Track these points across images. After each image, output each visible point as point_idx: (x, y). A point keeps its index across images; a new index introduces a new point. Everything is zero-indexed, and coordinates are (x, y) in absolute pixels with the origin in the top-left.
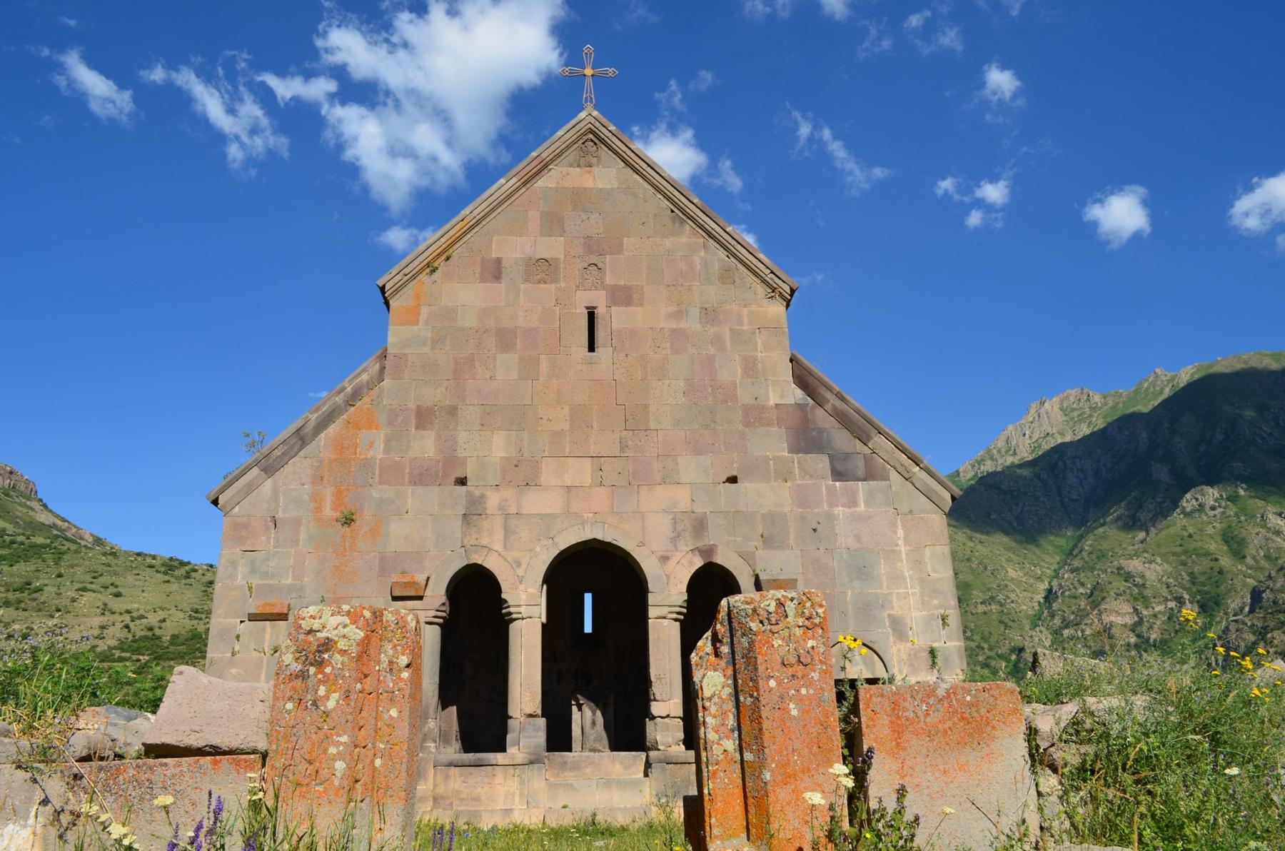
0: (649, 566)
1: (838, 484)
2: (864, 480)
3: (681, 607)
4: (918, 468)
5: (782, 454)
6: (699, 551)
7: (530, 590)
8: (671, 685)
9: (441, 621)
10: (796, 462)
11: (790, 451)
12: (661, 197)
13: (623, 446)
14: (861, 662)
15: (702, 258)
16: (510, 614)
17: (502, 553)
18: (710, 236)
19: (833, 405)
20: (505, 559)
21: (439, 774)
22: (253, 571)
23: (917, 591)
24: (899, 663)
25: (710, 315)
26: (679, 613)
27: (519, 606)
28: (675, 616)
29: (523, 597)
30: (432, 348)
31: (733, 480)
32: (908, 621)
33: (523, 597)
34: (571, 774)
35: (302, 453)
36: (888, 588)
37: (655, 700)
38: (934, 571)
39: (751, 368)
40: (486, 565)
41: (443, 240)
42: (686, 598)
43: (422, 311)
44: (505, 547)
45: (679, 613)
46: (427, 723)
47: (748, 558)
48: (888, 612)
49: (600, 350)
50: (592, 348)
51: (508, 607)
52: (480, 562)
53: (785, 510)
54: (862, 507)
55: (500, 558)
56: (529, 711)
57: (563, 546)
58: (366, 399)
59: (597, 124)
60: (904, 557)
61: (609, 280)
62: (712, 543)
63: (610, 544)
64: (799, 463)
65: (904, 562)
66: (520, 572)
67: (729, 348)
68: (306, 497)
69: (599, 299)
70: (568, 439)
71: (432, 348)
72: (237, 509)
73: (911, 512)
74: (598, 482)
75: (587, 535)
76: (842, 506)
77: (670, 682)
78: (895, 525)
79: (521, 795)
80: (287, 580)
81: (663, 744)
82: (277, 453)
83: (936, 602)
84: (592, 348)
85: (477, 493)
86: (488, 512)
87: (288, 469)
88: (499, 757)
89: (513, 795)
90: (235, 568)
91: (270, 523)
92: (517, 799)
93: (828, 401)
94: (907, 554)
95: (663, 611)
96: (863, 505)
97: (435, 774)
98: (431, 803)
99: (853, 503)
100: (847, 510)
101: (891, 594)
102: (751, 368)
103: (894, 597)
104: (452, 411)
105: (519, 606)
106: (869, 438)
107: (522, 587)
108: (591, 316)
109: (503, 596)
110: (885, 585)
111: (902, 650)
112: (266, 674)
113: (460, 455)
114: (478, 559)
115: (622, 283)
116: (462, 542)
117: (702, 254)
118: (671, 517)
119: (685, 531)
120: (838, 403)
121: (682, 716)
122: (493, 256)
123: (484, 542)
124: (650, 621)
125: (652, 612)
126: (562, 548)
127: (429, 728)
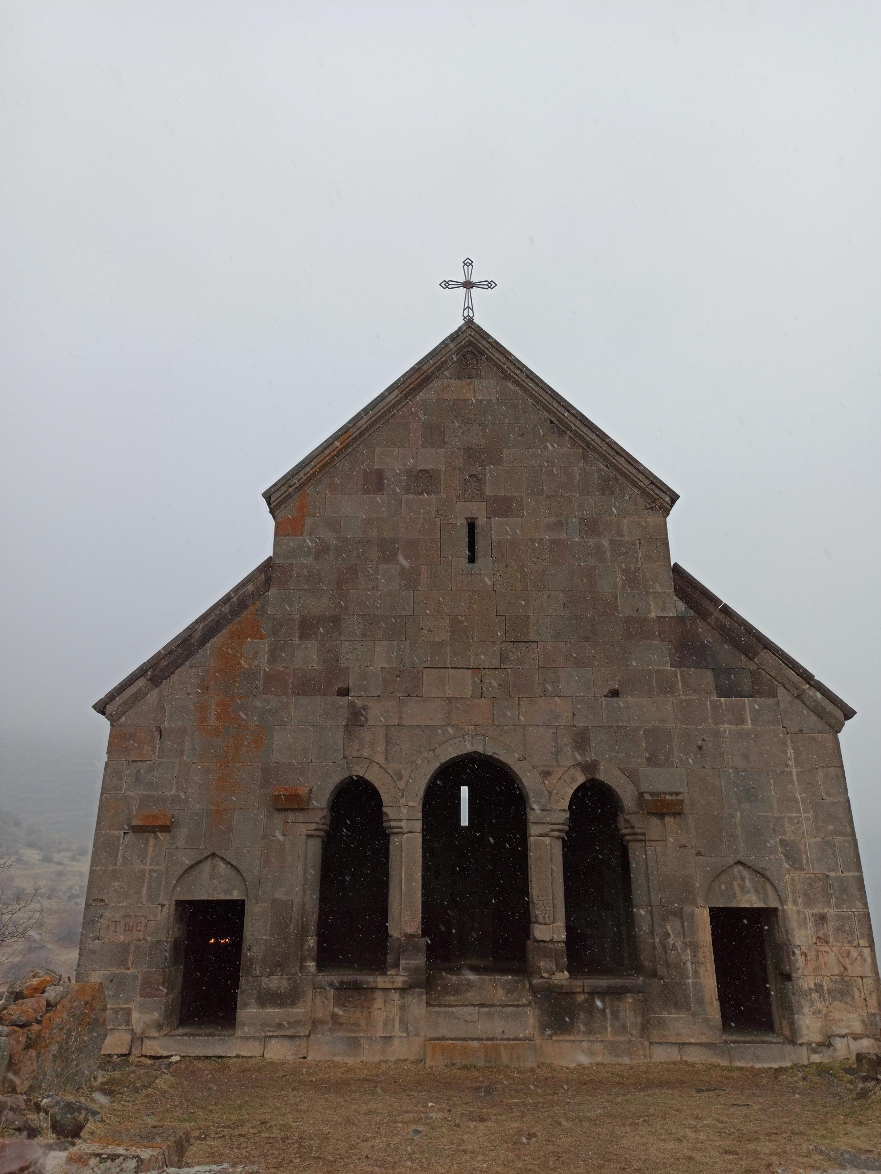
0: (529, 780)
1: (722, 699)
2: (751, 696)
3: (563, 824)
4: (807, 686)
5: (664, 668)
7: (411, 804)
8: (554, 908)
10: (679, 677)
11: (672, 666)
12: (540, 408)
13: (504, 658)
14: (752, 891)
15: (581, 468)
16: (391, 828)
17: (383, 765)
18: (589, 447)
19: (717, 619)
20: (387, 772)
21: (318, 997)
22: (138, 780)
23: (811, 815)
24: (794, 892)
25: (590, 526)
28: (557, 834)
29: (405, 811)
30: (316, 558)
31: (615, 693)
32: (802, 847)
33: (405, 811)
34: (452, 998)
35: (187, 663)
36: (780, 812)
37: (537, 922)
38: (828, 794)
39: (632, 579)
40: (367, 777)
41: (327, 452)
42: (568, 816)
43: (307, 522)
44: (386, 759)
45: (560, 831)
46: (307, 941)
47: (632, 776)
48: (780, 837)
49: (480, 561)
50: (472, 559)
51: (390, 820)
53: (669, 726)
54: (749, 725)
56: (410, 931)
57: (444, 758)
58: (251, 609)
59: (477, 336)
60: (795, 778)
61: (489, 491)
63: (491, 757)
64: (681, 677)
65: (796, 784)
66: (401, 785)
67: (609, 559)
68: (192, 707)
69: (479, 511)
70: (448, 649)
71: (315, 559)
72: (123, 719)
73: (801, 731)
74: (479, 694)
75: (468, 747)
76: (729, 723)
78: (784, 744)
79: (402, 1021)
80: (171, 790)
81: (547, 972)
82: (164, 663)
83: (831, 828)
84: (472, 559)
85: (359, 703)
86: (370, 722)
87: (175, 677)
88: (381, 981)
89: (394, 1019)
90: (120, 779)
91: (156, 733)
92: (397, 1025)
93: (711, 614)
94: (797, 775)
95: (546, 829)
96: (750, 722)
99: (741, 720)
100: (733, 727)
101: (783, 818)
102: (632, 579)
103: (786, 820)
104: (336, 621)
105: (400, 820)
106: (756, 654)
107: (403, 801)
108: (472, 527)
109: (384, 809)
110: (776, 807)
111: (797, 879)
112: (149, 888)
113: (342, 666)
114: (359, 771)
115: (502, 494)
117: (582, 465)
118: (552, 731)
119: (566, 745)
120: (722, 617)
122: (377, 467)
124: (532, 838)
125: (533, 830)
126: (443, 761)
127: (309, 946)
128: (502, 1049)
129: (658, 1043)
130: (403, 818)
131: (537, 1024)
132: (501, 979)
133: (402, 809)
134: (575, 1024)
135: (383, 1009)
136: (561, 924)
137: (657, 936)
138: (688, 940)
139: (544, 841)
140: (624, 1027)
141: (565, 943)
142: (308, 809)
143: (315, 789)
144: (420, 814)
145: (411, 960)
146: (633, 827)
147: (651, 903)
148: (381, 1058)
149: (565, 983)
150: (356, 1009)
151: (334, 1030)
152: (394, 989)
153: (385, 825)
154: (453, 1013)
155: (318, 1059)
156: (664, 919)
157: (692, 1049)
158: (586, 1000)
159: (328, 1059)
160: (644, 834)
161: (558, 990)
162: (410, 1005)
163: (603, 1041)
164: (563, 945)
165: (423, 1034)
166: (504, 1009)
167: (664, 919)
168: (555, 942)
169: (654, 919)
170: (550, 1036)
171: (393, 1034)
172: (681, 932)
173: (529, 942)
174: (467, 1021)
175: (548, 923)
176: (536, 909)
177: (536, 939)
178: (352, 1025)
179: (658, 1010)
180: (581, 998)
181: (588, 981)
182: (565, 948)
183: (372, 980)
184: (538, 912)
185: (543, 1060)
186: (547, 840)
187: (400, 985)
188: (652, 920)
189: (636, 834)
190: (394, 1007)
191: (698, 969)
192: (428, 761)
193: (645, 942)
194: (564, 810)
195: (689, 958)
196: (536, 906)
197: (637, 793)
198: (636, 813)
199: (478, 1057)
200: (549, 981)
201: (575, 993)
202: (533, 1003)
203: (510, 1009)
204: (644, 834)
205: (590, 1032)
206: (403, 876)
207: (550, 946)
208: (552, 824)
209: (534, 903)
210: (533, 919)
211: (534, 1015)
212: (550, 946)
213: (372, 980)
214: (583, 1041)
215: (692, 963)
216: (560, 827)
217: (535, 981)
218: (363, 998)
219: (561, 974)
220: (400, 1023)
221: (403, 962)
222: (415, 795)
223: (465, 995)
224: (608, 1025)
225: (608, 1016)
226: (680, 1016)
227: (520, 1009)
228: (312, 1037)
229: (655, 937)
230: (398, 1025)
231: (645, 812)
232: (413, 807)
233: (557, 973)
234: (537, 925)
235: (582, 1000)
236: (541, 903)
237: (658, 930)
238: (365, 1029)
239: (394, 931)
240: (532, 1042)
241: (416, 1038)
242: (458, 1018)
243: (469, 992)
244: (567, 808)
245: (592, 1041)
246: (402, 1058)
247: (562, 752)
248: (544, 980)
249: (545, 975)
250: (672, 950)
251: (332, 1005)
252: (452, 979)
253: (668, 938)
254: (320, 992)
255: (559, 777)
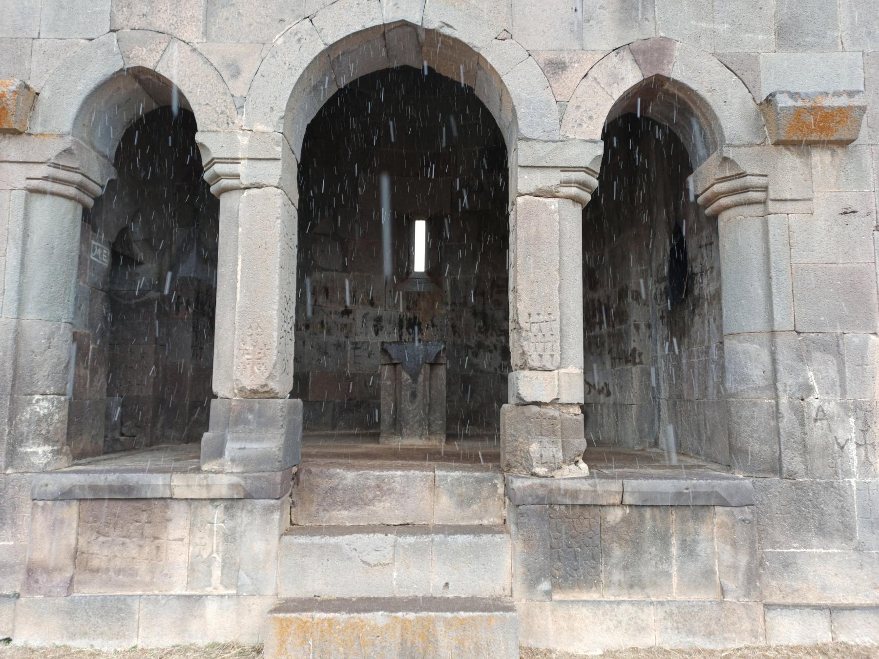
3: (587, 170)
6: (632, 52)
7: (259, 127)
8: (562, 337)
9: (72, 191)
16: (217, 177)
17: (197, 46)
20: (207, 61)
21: (40, 517)
26: (583, 185)
27: (235, 160)
28: (573, 191)
34: (345, 513)
40: (161, 70)
42: (600, 151)
44: (205, 34)
45: (583, 185)
51: (212, 162)
52: (149, 65)
55: (195, 56)
56: (249, 383)
62: (662, 34)
66: (238, 87)
77: (561, 330)
81: (543, 464)
92: (217, 573)
95: (552, 179)
97: (33, 514)
98: (22, 576)
105: (235, 160)
107: (241, 120)
109: (199, 138)
116: (112, 20)
119: (601, 7)
121: (582, 402)
123: (161, 23)
128: (441, 628)
129: (785, 606)
130: (240, 156)
131: (520, 570)
132: (446, 477)
133: (239, 137)
134: (602, 568)
135: (186, 540)
136: (575, 369)
137: (785, 391)
138: (850, 399)
139: (545, 204)
140: (708, 574)
141: (585, 408)
142: (30, 134)
143: (45, 94)
144: (278, 151)
145: (252, 441)
146: (742, 175)
147: (772, 325)
148: (176, 641)
149: (585, 486)
150: (127, 540)
151: (80, 583)
152: (213, 500)
153: (206, 176)
154: (337, 546)
155: (34, 643)
156: (802, 357)
157: (858, 618)
158: (625, 520)
159: (58, 643)
160: (765, 189)
161: (568, 501)
162: (245, 531)
163: (662, 603)
164: (578, 411)
165: (270, 591)
166: (450, 539)
167: (800, 358)
168: (562, 404)
169: (780, 357)
170: (548, 593)
171: (209, 590)
172: (838, 383)
173: (505, 406)
174: (369, 564)
175: (549, 366)
176: (527, 339)
177: (521, 399)
178: (119, 571)
179: (782, 538)
180: (615, 515)
181: (634, 483)
182: (581, 417)
183: (160, 483)
184: (528, 347)
185: (532, 643)
186: (553, 204)
187: (225, 493)
188: (774, 361)
189: (745, 189)
190: (211, 535)
191: (872, 459)
192: (299, 40)
193: (755, 404)
194: (594, 142)
195: (854, 435)
196: (524, 334)
197: (752, 105)
198: (750, 145)
199: (384, 647)
200: (548, 482)
201: (602, 506)
202: (513, 528)
203: (461, 539)
204: (765, 189)
205: (634, 584)
206: (239, 273)
207: (551, 411)
208: (565, 169)
209: (521, 328)
210: (515, 359)
211: (514, 548)
212: (551, 411)
213: (160, 483)
214: (619, 603)
215: (858, 445)
216: (582, 176)
217: (518, 484)
218: (144, 517)
219: (573, 467)
220: (223, 567)
221: (231, 447)
222: (268, 110)
223: (371, 507)
224: (674, 570)
225: (674, 550)
226: (830, 551)
227: (486, 538)
228: (22, 600)
229: (781, 393)
230: (219, 573)
231: (769, 142)
232: (263, 133)
233: (564, 466)
234: (526, 372)
235: (618, 520)
236: (535, 328)
237: (786, 380)
238: (148, 579)
239: (220, 385)
240: (508, 615)
241: (256, 600)
242: (349, 558)
243: (380, 501)
244: (598, 135)
245: (639, 602)
246: (222, 640)
247: (592, 22)
248: (537, 481)
249: (541, 470)
250: (816, 420)
251: (74, 532)
252: (343, 478)
253: (808, 397)
254: (43, 508)
255: (583, 75)
